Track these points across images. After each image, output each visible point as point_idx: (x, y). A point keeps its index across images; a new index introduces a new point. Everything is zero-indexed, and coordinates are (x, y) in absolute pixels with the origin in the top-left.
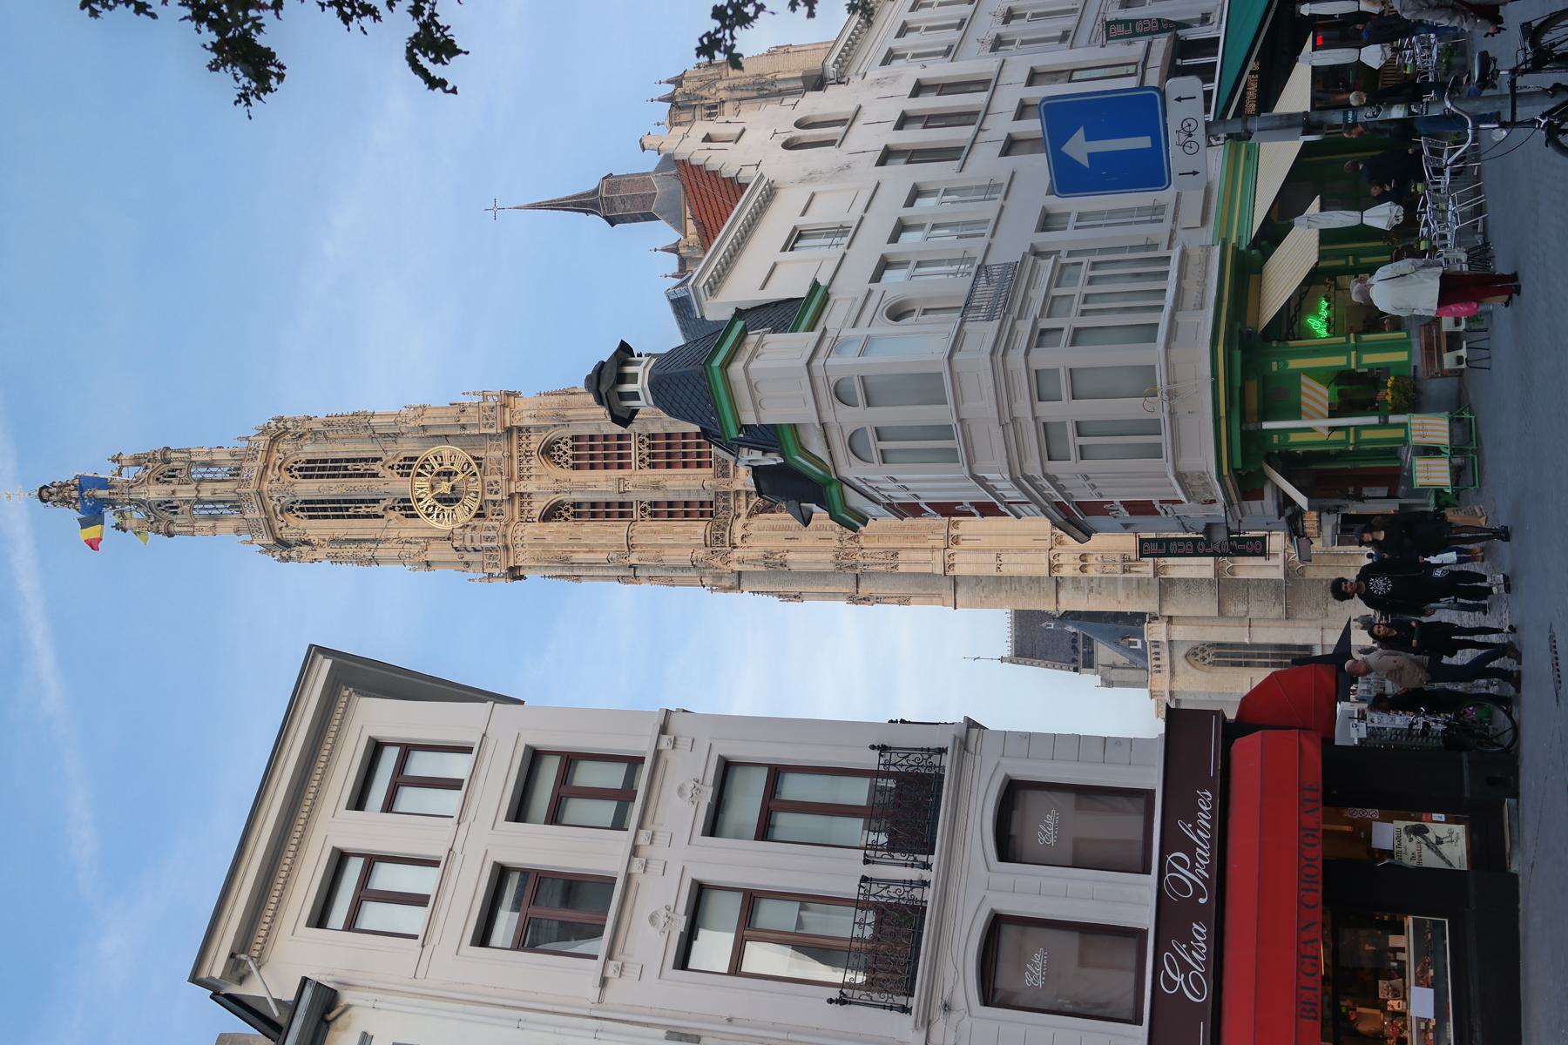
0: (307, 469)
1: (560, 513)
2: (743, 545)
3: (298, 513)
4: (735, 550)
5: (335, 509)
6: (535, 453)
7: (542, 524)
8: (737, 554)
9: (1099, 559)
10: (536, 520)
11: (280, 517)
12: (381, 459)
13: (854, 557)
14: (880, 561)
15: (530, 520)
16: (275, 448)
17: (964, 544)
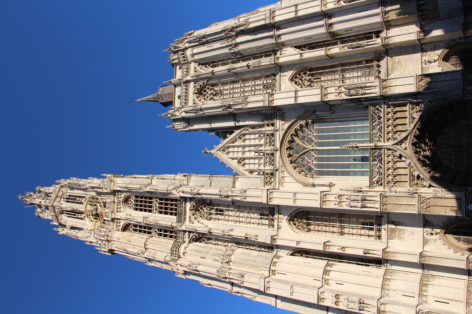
0: (69, 199)
1: (129, 228)
2: (184, 257)
3: (65, 214)
4: (179, 259)
5: (73, 215)
6: (121, 202)
7: (122, 232)
8: (180, 261)
9: (346, 299)
10: (120, 230)
11: (60, 215)
12: (85, 197)
13: (225, 273)
14: (236, 278)
15: (118, 230)
16: (61, 190)
17: (278, 276)
